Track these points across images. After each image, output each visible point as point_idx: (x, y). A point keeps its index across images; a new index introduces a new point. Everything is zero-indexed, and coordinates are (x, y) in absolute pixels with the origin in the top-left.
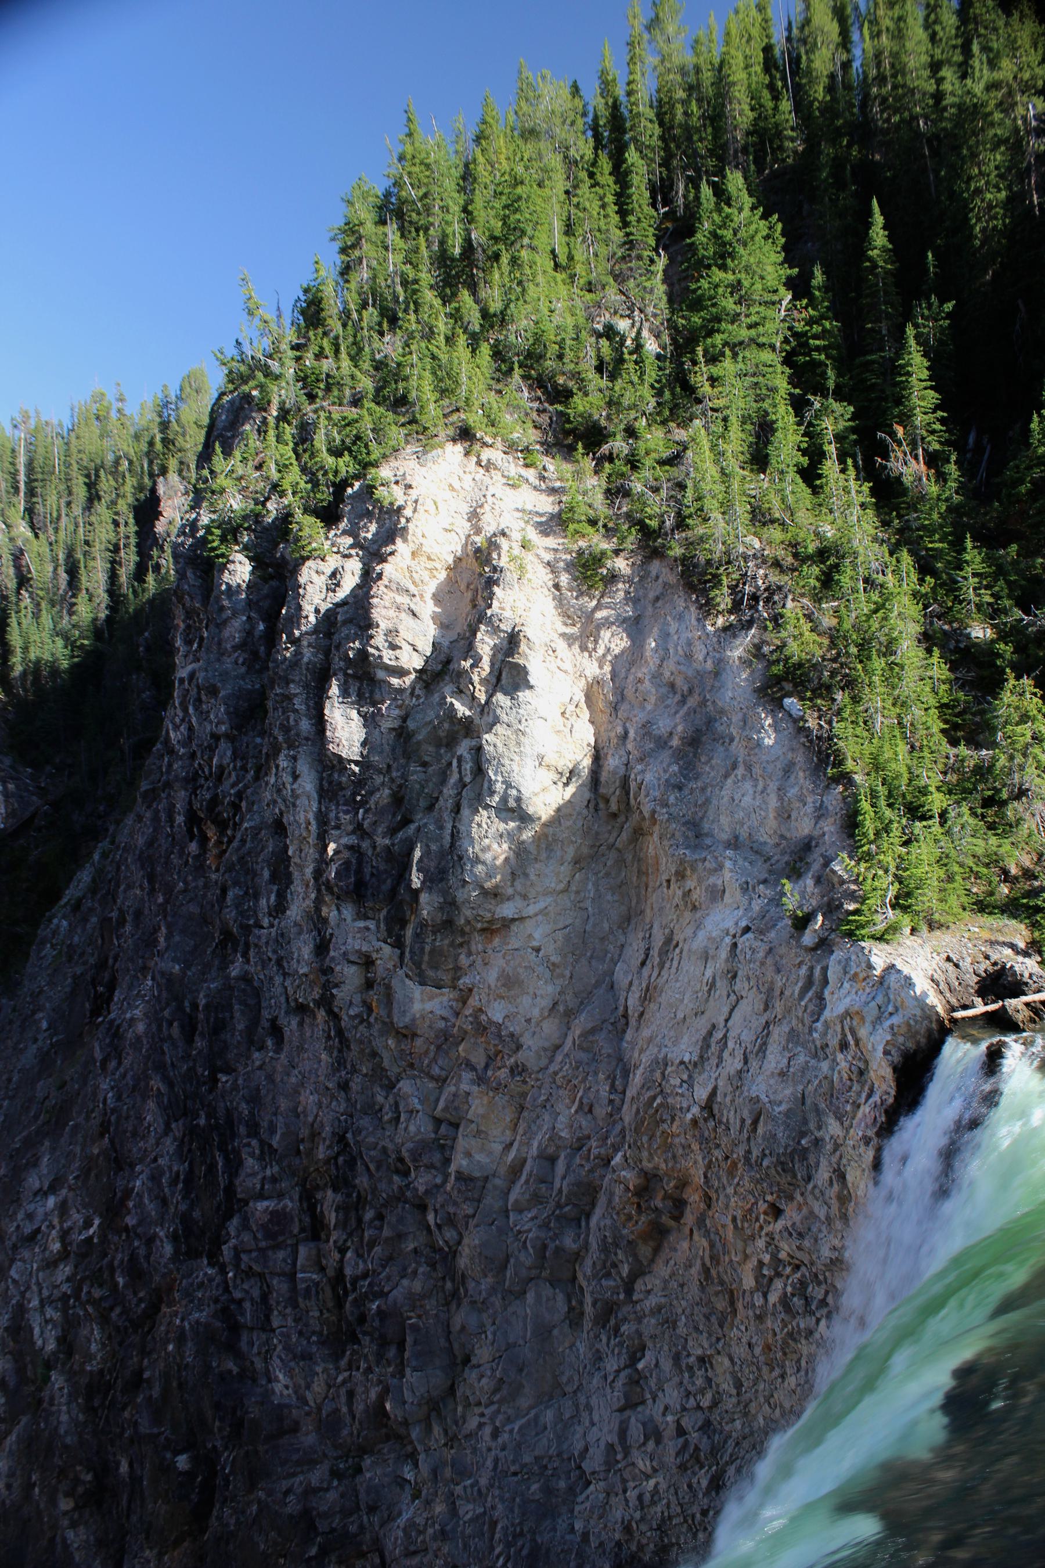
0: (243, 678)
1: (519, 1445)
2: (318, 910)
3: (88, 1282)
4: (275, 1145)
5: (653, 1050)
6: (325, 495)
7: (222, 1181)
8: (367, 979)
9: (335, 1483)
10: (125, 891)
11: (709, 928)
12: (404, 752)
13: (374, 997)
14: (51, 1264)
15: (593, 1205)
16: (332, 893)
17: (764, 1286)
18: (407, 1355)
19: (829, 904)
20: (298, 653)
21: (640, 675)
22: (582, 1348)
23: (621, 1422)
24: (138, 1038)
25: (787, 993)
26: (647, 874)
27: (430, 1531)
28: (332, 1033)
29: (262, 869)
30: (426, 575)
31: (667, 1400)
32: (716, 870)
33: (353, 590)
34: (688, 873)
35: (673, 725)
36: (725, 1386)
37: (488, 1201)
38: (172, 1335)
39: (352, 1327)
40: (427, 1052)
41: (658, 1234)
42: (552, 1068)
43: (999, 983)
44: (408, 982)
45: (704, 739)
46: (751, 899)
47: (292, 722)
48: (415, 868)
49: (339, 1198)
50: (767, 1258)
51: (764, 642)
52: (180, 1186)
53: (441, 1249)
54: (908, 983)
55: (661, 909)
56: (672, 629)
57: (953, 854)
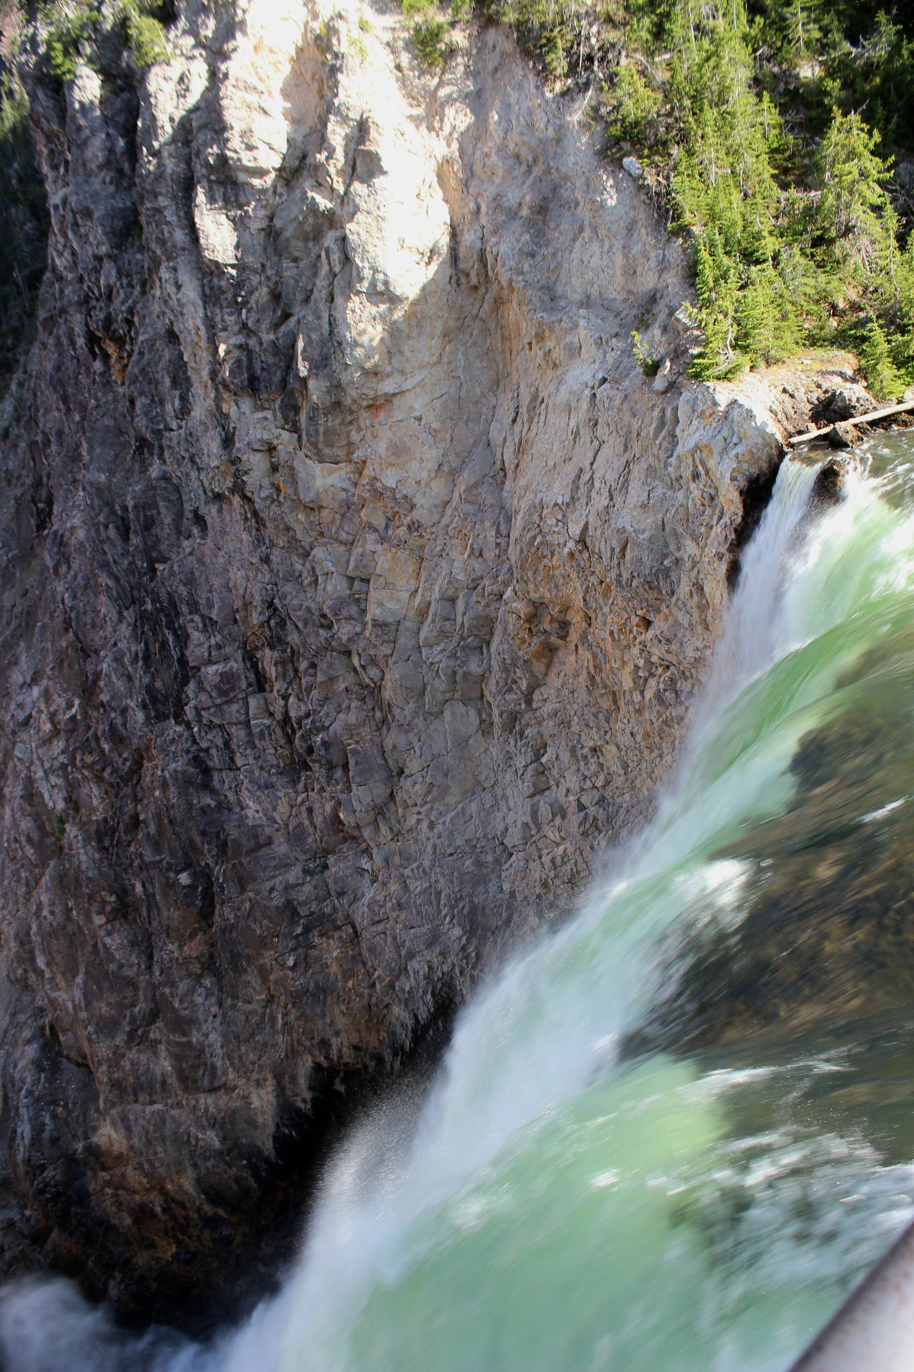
0: (113, 197)
1: (452, 833)
2: (219, 407)
3: (80, 752)
4: (215, 618)
5: (530, 496)
8: (272, 463)
9: (308, 879)
10: (44, 415)
11: (570, 382)
12: (275, 250)
13: (279, 478)
14: (47, 742)
15: (492, 634)
16: (230, 391)
17: (640, 685)
18: (351, 774)
19: (675, 350)
21: (486, 150)
22: (494, 751)
23: (533, 805)
24: (81, 544)
25: (643, 434)
26: (511, 341)
27: (389, 905)
28: (249, 515)
29: (163, 377)
31: (568, 784)
32: (572, 329)
33: (203, 95)
34: (547, 333)
35: (522, 195)
36: (614, 768)
37: (402, 641)
38: (156, 784)
39: (303, 757)
40: (333, 521)
41: (549, 651)
42: (445, 521)
44: (307, 460)
45: (551, 206)
46: (605, 352)
47: (166, 235)
48: (300, 358)
49: (276, 654)
50: (641, 662)
51: (600, 104)
52: (141, 663)
53: (368, 686)
54: (750, 415)
55: (526, 370)
56: (513, 101)
57: (786, 294)
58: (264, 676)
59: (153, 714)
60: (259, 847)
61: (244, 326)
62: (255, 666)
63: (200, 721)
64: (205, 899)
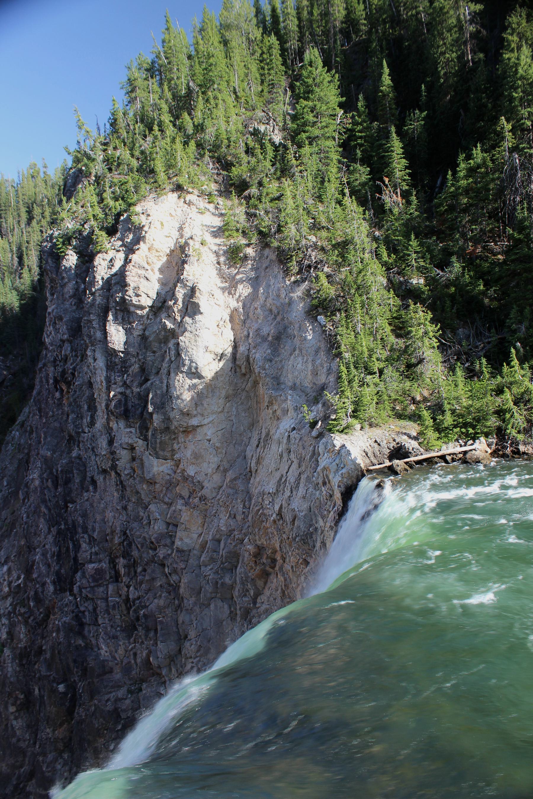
0: (74, 312)
3: (19, 606)
4: (95, 537)
6: (111, 220)
7: (72, 554)
8: (132, 456)
9: (130, 696)
10: (32, 417)
12: (145, 346)
13: (135, 465)
15: (238, 562)
16: (114, 416)
18: (158, 635)
20: (94, 300)
24: (36, 488)
30: (155, 260)
34: (274, 402)
37: (191, 561)
38: (54, 629)
39: (136, 623)
40: (162, 491)
41: (265, 575)
43: (399, 452)
44: (151, 457)
45: (282, 336)
47: (92, 333)
53: (173, 585)
54: (349, 453)
55: (265, 419)
56: (272, 284)
58: (119, 573)
59: (58, 587)
60: (105, 673)
61: (125, 383)
62: (115, 567)
63: (81, 595)
64: (71, 701)
